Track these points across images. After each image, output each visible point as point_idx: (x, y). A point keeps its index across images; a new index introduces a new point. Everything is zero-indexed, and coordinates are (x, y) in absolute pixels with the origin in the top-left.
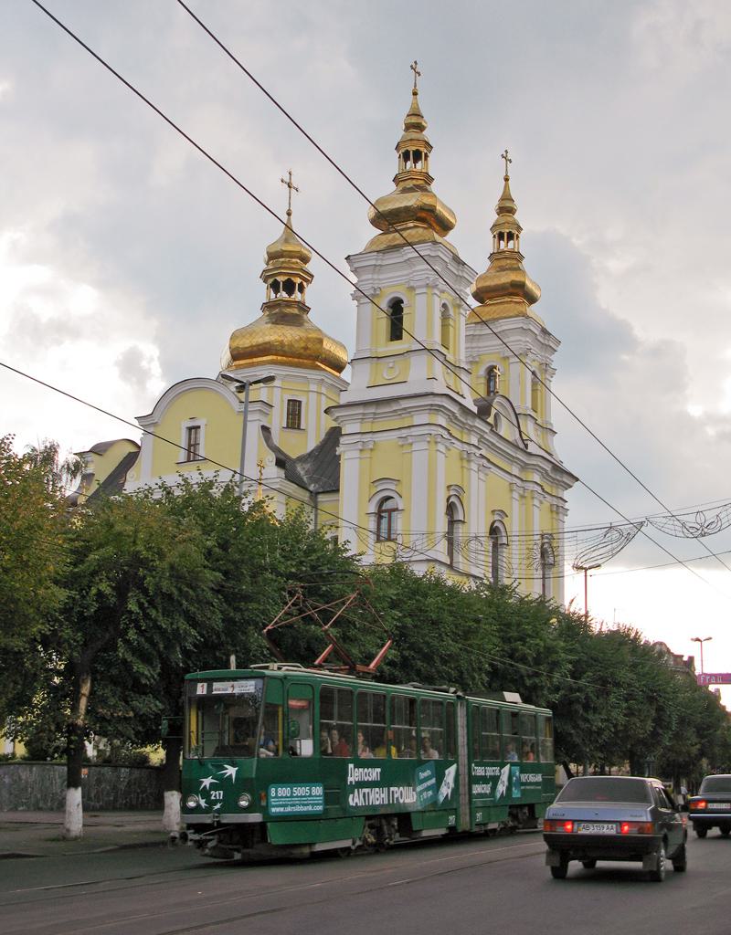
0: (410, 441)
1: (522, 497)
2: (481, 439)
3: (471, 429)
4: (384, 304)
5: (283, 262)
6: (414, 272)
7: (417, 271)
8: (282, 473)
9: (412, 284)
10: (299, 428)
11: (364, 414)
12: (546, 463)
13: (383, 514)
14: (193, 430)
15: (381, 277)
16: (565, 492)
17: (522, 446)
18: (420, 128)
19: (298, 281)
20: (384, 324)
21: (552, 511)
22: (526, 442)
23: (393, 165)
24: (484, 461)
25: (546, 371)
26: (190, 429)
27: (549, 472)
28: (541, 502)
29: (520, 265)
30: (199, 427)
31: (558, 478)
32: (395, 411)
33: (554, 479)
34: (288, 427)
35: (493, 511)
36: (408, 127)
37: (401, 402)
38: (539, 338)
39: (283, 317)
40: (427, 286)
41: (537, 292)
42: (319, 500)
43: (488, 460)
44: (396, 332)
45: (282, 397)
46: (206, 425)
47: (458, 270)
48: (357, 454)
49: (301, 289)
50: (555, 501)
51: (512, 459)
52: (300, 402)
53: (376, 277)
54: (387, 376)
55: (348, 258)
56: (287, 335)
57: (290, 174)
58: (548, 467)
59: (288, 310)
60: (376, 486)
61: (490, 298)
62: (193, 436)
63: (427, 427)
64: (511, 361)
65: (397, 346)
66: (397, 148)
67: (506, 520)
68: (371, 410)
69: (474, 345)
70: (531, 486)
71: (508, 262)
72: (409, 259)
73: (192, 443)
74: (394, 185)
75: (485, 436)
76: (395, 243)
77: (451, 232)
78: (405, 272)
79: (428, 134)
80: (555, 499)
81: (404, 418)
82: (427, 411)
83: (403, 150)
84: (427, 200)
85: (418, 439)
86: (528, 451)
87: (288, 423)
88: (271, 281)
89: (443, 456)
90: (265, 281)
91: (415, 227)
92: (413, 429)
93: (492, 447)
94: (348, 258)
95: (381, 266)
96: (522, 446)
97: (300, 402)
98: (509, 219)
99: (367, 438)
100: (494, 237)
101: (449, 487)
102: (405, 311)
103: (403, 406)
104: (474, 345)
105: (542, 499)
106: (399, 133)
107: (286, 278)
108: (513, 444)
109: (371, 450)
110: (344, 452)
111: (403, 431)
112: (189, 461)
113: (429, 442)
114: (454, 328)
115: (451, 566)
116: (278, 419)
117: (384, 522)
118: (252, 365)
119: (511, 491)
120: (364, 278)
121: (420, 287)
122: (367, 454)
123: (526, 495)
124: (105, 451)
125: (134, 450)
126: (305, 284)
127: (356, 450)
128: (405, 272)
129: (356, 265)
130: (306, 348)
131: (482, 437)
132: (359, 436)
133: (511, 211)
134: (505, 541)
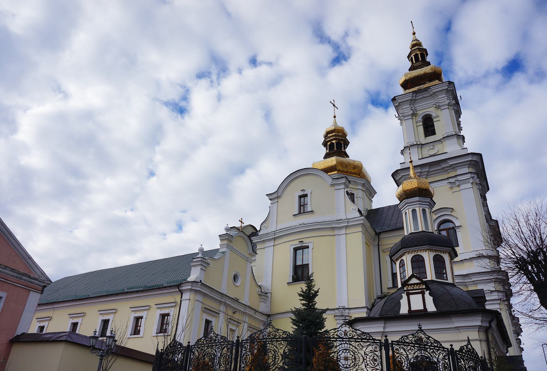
4: (420, 119)
6: (438, 99)
11: (421, 172)
14: (303, 196)
18: (419, 44)
19: (342, 142)
20: (421, 129)
26: (300, 197)
30: (306, 196)
32: (443, 168)
37: (448, 161)
46: (311, 193)
49: (345, 148)
52: (354, 194)
54: (432, 152)
57: (334, 100)
63: (470, 175)
66: (408, 57)
72: (434, 93)
73: (302, 204)
78: (433, 101)
88: (329, 143)
92: (458, 177)
97: (354, 194)
102: (434, 120)
103: (450, 164)
107: (337, 141)
112: (300, 213)
125: (254, 231)
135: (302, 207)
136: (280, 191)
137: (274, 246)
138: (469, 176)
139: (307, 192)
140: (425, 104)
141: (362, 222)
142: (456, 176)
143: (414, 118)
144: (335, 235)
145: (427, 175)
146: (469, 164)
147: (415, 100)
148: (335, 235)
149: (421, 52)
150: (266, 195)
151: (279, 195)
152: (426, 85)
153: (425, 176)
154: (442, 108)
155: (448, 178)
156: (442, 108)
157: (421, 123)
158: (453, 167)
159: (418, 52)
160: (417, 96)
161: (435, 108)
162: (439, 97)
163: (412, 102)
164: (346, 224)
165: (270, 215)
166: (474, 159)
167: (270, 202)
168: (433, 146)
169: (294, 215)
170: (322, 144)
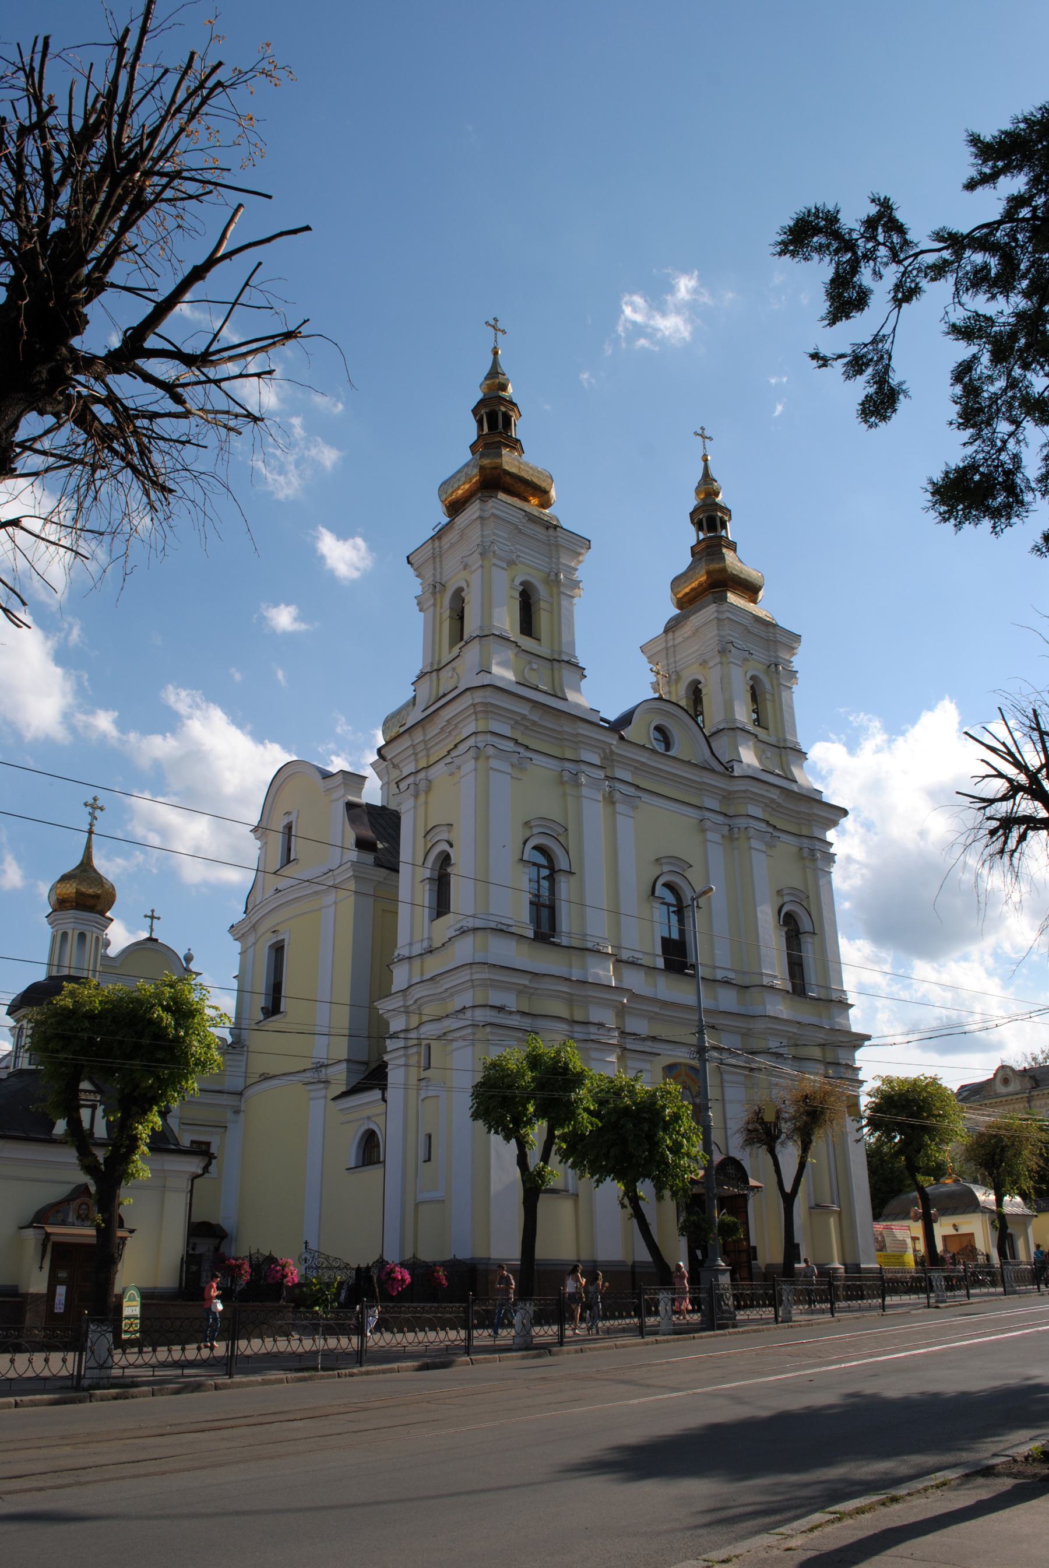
8: (369, 858)
11: (413, 746)
12: (772, 789)
24: (618, 785)
27: (780, 801)
28: (767, 844)
31: (803, 809)
32: (442, 729)
33: (798, 813)
37: (443, 713)
44: (458, 634)
50: (806, 843)
68: (418, 736)
70: (742, 822)
80: (806, 841)
86: (736, 774)
93: (639, 768)
102: (466, 601)
108: (705, 768)
112: (287, 864)
114: (551, 612)
119: (703, 831)
122: (422, 798)
138: (471, 742)
139: (292, 818)
141: (351, 874)
144: (320, 909)
145: (428, 750)
147: (441, 557)
148: (320, 909)
153: (424, 753)
157: (447, 614)
166: (476, 701)
167: (258, 843)
168: (454, 669)
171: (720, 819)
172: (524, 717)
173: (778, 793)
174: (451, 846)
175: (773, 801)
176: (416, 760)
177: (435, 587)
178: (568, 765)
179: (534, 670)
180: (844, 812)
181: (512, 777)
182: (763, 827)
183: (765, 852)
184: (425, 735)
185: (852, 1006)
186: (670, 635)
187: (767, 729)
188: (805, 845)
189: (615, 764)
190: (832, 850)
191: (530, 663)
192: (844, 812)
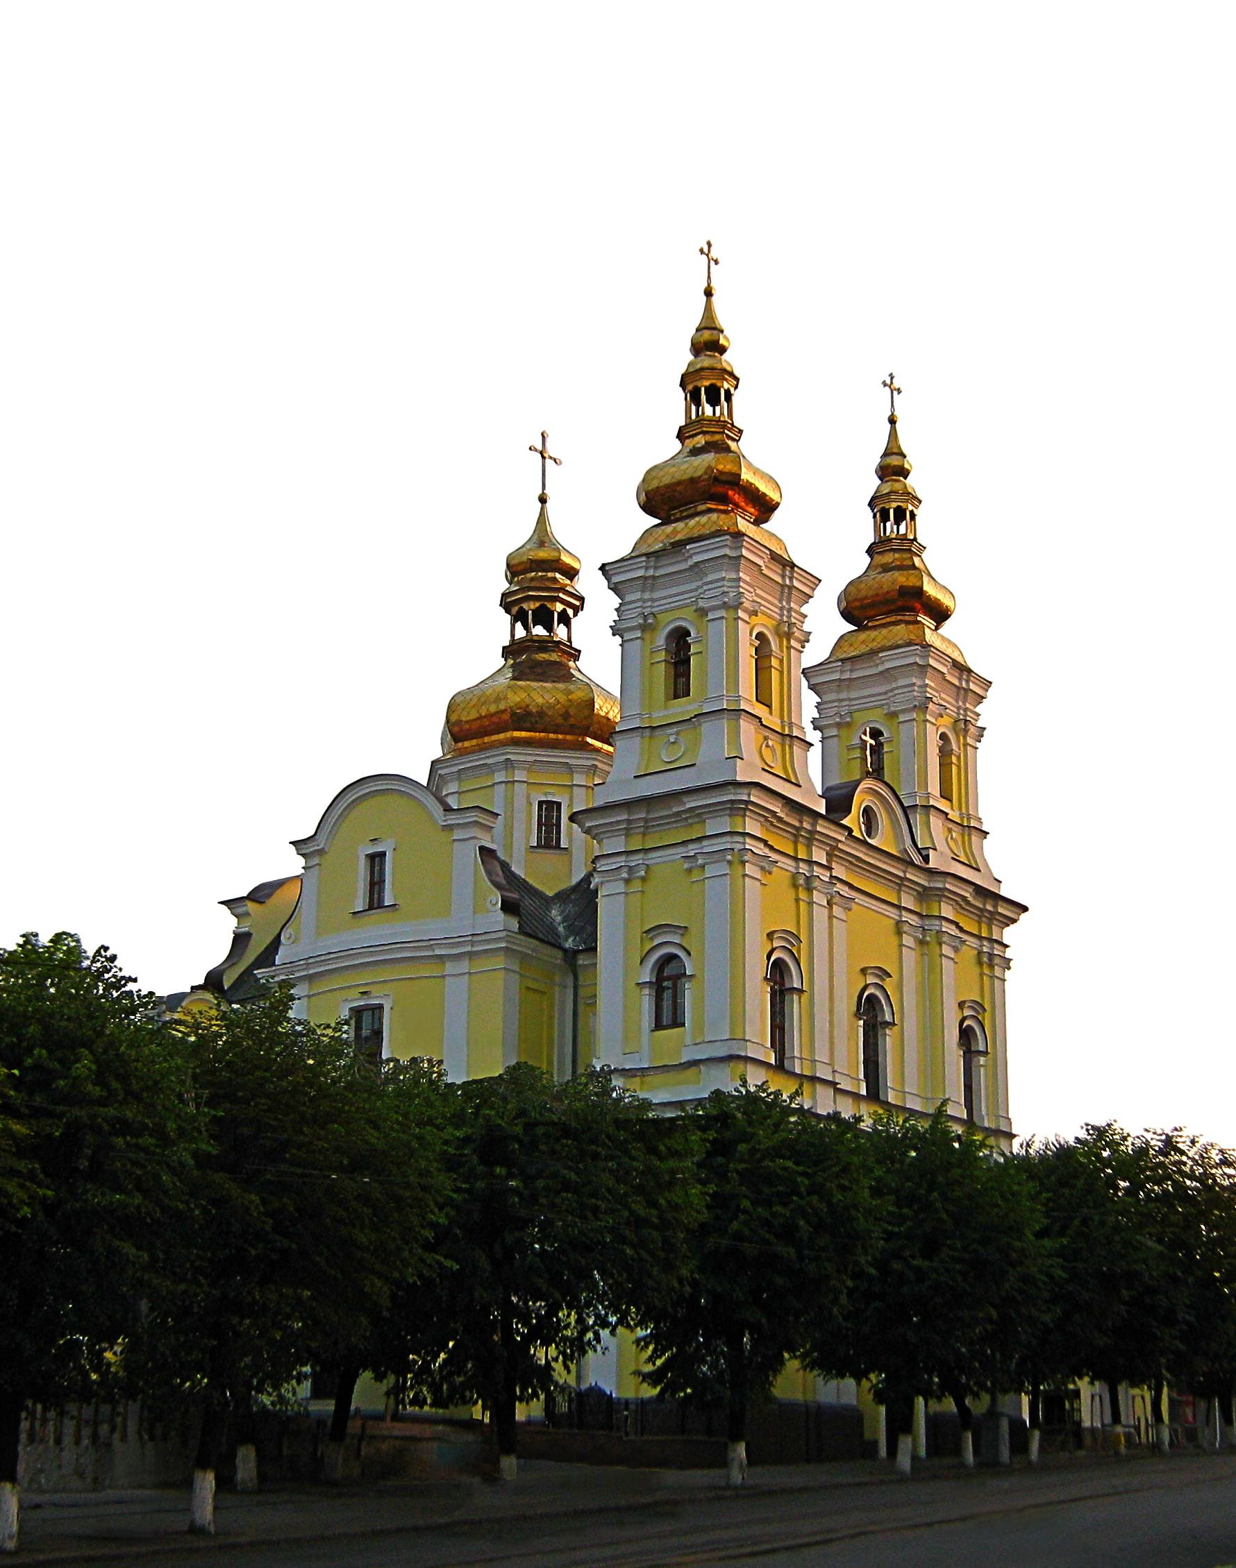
0: (700, 861)
1: (922, 943)
2: (833, 852)
3: (811, 838)
4: (661, 640)
5: (532, 579)
7: (711, 582)
8: (514, 924)
9: (701, 604)
10: (558, 846)
11: (629, 821)
13: (665, 984)
14: (377, 859)
15: (657, 595)
16: (1006, 931)
17: (917, 860)
21: (980, 963)
22: (924, 853)
23: (675, 410)
24: (839, 887)
25: (966, 731)
27: (970, 899)
28: (956, 950)
29: (916, 560)
30: (383, 854)
31: (989, 907)
32: (678, 814)
34: (539, 846)
35: (864, 971)
36: (698, 348)
38: (948, 677)
39: (531, 667)
40: (725, 606)
41: (946, 601)
42: (581, 962)
43: (851, 886)
44: (680, 685)
45: (528, 797)
47: (783, 577)
48: (621, 887)
49: (565, 620)
51: (901, 884)
53: (647, 596)
55: (603, 568)
56: (541, 694)
58: (967, 893)
59: (542, 656)
60: (652, 939)
61: (871, 619)
62: (377, 868)
63: (728, 839)
64: (901, 719)
65: (683, 708)
67: (889, 984)
69: (843, 696)
71: (897, 555)
72: (696, 563)
74: (677, 441)
75: (840, 846)
76: (677, 538)
77: (777, 514)
78: (693, 586)
79: (731, 359)
81: (691, 825)
82: (728, 812)
83: (690, 387)
84: (724, 465)
85: (716, 856)
86: (931, 865)
87: (539, 838)
88: (515, 610)
89: (758, 883)
90: (508, 611)
91: (710, 511)
92: (705, 843)
93: (854, 863)
94: (603, 568)
95: (654, 577)
96: (917, 860)
97: (559, 805)
98: (897, 486)
99: (636, 860)
100: (875, 516)
101: (770, 936)
103: (688, 806)
104: (843, 696)
105: (957, 943)
106: (683, 358)
107: (537, 604)
109: (643, 879)
110: (602, 883)
111: (691, 846)
113: (730, 862)
115: (780, 1067)
116: (527, 831)
117: (667, 995)
118: (483, 748)
119: (899, 933)
120: (628, 598)
121: (714, 608)
122: (636, 886)
123: (928, 938)
124: (270, 895)
126: (570, 612)
127: (621, 879)
128: (693, 586)
129: (615, 579)
130: (566, 715)
131: (836, 848)
132: (623, 858)
133: (905, 473)
134: (888, 1018)
135: (376, 888)
136: (321, 843)
137: (309, 997)
140: (681, 594)
141: (503, 945)
142: (699, 839)
143: (647, 636)
144: (443, 977)
145: (647, 828)
146: (730, 808)
148: (443, 977)
149: (707, 383)
150: (291, 843)
151: (321, 847)
152: (692, 522)
153: (642, 830)
154: (711, 616)
155: (684, 842)
156: (711, 616)
158: (699, 815)
159: (699, 384)
160: (659, 564)
161: (695, 611)
162: (710, 578)
163: (647, 583)
164: (469, 949)
165: (304, 904)
167: (301, 861)
169: (354, 913)
170: (501, 605)
171: (914, 920)
172: (774, 813)
173: (971, 890)
174: (689, 954)
175: (964, 898)
176: (627, 835)
177: (645, 617)
178: (803, 868)
179: (767, 746)
180: (1025, 909)
181: (762, 884)
182: (953, 931)
183: (952, 959)
184: (648, 812)
185: (1015, 1136)
186: (848, 666)
187: (950, 800)
188: (985, 949)
189: (834, 859)
190: (1009, 954)
191: (766, 738)
192: (1025, 909)
